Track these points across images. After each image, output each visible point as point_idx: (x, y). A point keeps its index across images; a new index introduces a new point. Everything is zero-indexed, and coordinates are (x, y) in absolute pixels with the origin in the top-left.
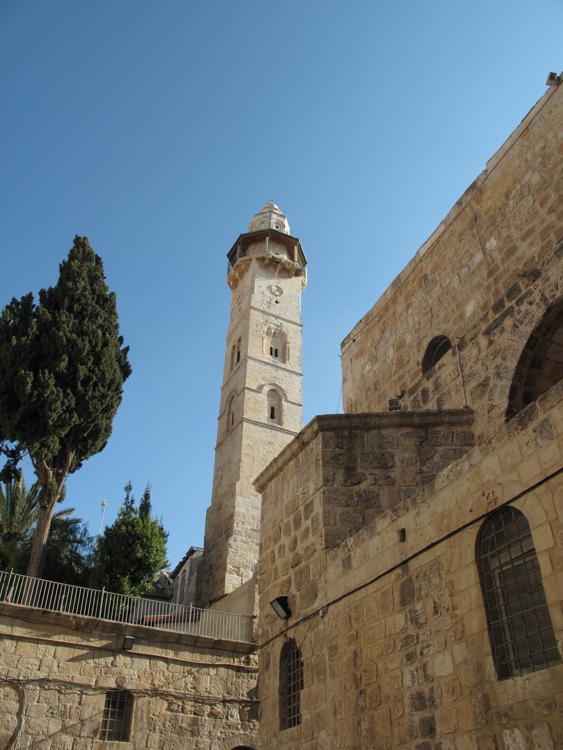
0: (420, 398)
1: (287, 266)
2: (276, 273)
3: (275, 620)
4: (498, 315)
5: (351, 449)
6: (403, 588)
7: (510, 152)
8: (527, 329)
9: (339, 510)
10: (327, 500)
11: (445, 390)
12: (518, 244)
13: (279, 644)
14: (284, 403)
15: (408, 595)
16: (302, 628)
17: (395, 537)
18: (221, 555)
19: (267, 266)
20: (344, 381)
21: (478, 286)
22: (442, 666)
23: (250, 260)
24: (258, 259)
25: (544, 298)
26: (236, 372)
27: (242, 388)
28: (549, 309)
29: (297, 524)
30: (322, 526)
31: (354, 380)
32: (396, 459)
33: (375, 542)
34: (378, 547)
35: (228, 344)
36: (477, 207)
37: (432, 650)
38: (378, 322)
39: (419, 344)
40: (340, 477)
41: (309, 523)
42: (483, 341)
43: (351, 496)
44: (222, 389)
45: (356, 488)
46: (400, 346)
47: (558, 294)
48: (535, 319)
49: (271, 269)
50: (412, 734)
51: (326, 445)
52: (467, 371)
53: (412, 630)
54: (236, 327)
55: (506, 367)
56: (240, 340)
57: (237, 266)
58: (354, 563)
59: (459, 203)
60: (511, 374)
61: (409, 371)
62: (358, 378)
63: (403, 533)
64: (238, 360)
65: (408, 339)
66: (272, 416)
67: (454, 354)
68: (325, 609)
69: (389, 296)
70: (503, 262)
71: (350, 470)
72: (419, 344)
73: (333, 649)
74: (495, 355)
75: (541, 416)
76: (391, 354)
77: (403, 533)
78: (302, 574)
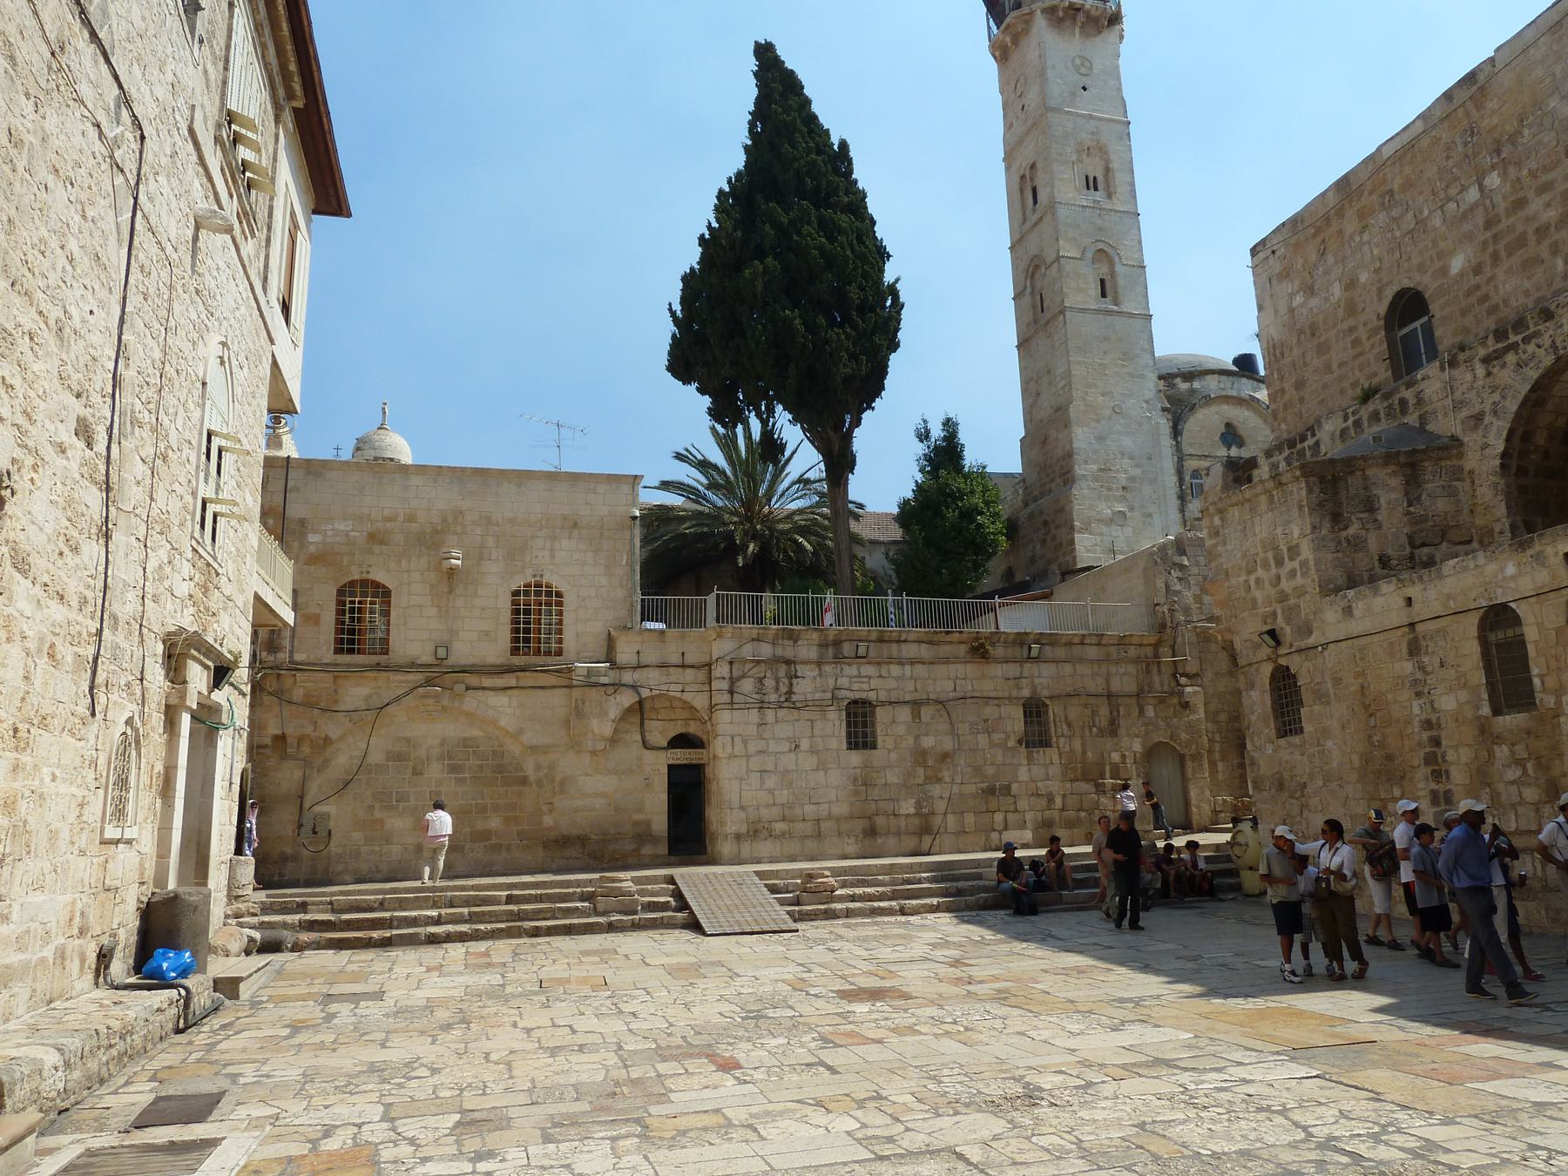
0: (1396, 406)
1: (1093, 12)
2: (1077, 31)
3: (1258, 646)
4: (1499, 346)
5: (1336, 493)
6: (1409, 643)
7: (1532, 51)
8: (1534, 375)
9: (1330, 557)
10: (1317, 549)
11: (1429, 408)
12: (1530, 194)
13: (1267, 669)
14: (1118, 268)
15: (1414, 649)
16: (1296, 657)
17: (1401, 603)
18: (1062, 510)
19: (1060, 21)
20: (1260, 308)
21: (1470, 237)
22: (1448, 703)
23: (1032, 13)
24: (1044, 11)
25: (1554, 346)
26: (1035, 225)
27: (1053, 257)
28: (1558, 359)
29: (1279, 562)
30: (1313, 571)
31: (1276, 312)
32: (1382, 501)
33: (1378, 602)
34: (1383, 605)
35: (1008, 169)
36: (1475, 114)
37: (1438, 692)
38: (1314, 236)
39: (1380, 291)
40: (1327, 525)
41: (1296, 564)
42: (1480, 371)
43: (1340, 542)
44: (1011, 248)
45: (1344, 534)
46: (1351, 285)
47: (1561, 421)
48: (1543, 365)
49: (1068, 23)
50: (1420, 745)
51: (1310, 491)
52: (1458, 395)
53: (1419, 675)
54: (1020, 142)
55: (1504, 407)
56: (1033, 166)
57: (1008, 26)
58: (1356, 613)
59: (1448, 96)
60: (1510, 417)
61: (1365, 325)
62: (1283, 310)
63: (1409, 601)
64: (1035, 202)
65: (1363, 278)
66: (1104, 295)
67: (1442, 369)
68: (1325, 646)
69: (1332, 200)
70: (1508, 216)
71: (1337, 518)
72: (1380, 291)
73: (1337, 681)
74: (1494, 389)
75: (1538, 548)
76: (1337, 291)
77: (1409, 601)
78: (1290, 613)
